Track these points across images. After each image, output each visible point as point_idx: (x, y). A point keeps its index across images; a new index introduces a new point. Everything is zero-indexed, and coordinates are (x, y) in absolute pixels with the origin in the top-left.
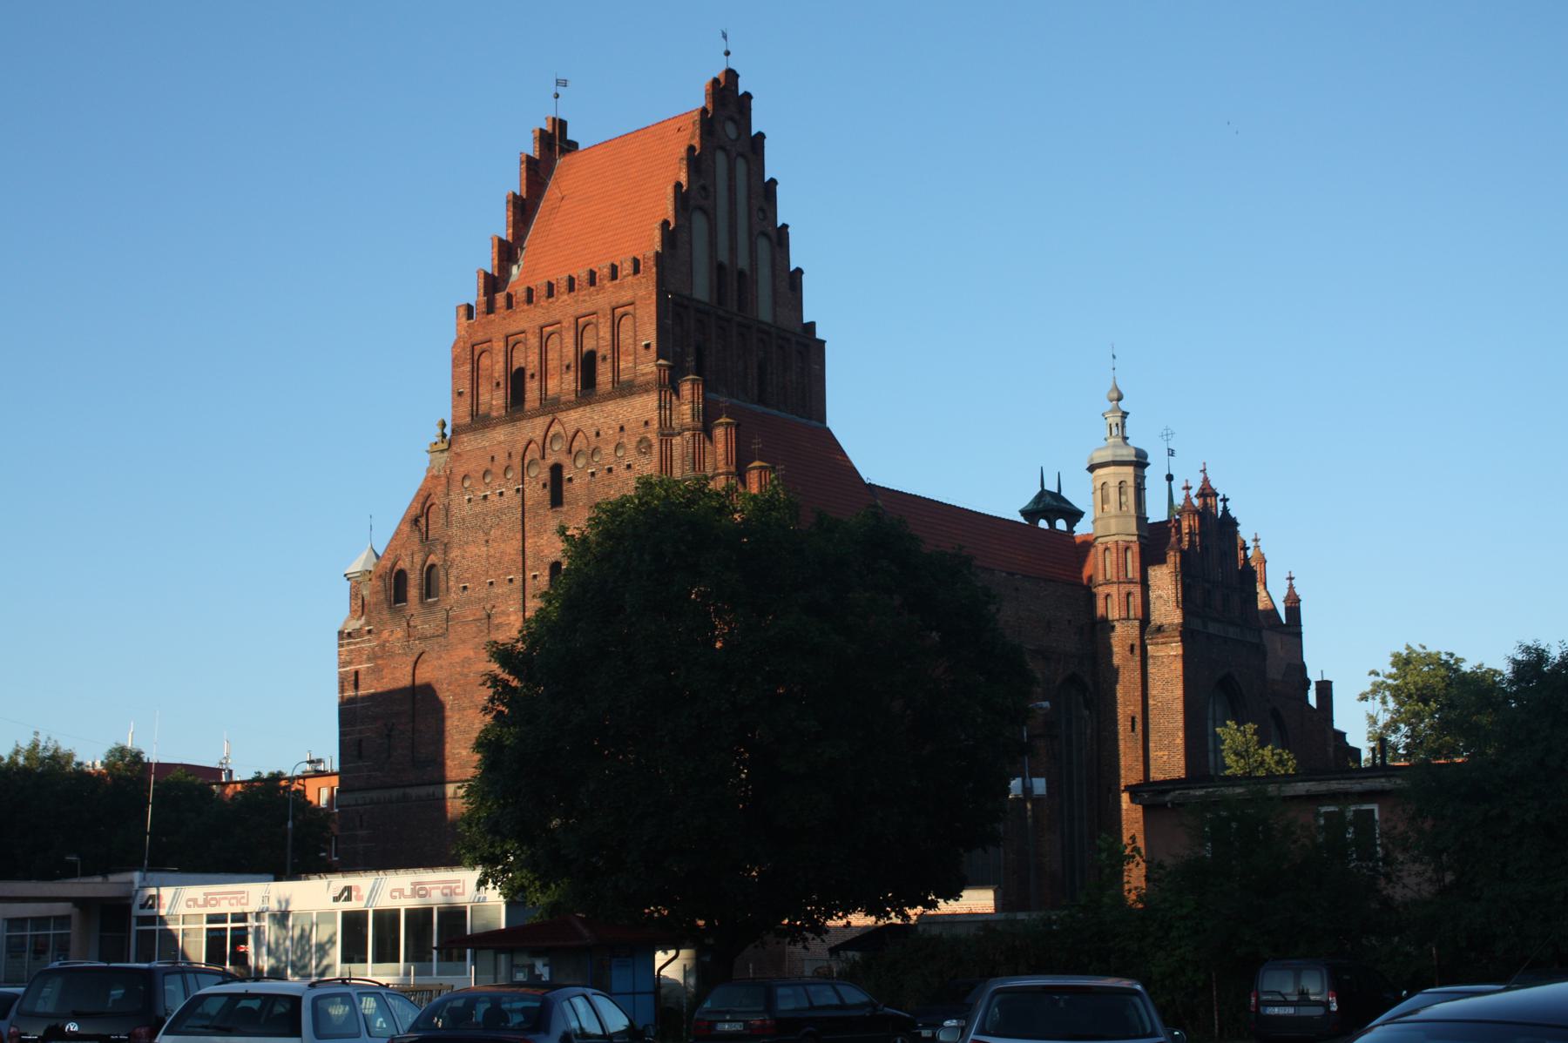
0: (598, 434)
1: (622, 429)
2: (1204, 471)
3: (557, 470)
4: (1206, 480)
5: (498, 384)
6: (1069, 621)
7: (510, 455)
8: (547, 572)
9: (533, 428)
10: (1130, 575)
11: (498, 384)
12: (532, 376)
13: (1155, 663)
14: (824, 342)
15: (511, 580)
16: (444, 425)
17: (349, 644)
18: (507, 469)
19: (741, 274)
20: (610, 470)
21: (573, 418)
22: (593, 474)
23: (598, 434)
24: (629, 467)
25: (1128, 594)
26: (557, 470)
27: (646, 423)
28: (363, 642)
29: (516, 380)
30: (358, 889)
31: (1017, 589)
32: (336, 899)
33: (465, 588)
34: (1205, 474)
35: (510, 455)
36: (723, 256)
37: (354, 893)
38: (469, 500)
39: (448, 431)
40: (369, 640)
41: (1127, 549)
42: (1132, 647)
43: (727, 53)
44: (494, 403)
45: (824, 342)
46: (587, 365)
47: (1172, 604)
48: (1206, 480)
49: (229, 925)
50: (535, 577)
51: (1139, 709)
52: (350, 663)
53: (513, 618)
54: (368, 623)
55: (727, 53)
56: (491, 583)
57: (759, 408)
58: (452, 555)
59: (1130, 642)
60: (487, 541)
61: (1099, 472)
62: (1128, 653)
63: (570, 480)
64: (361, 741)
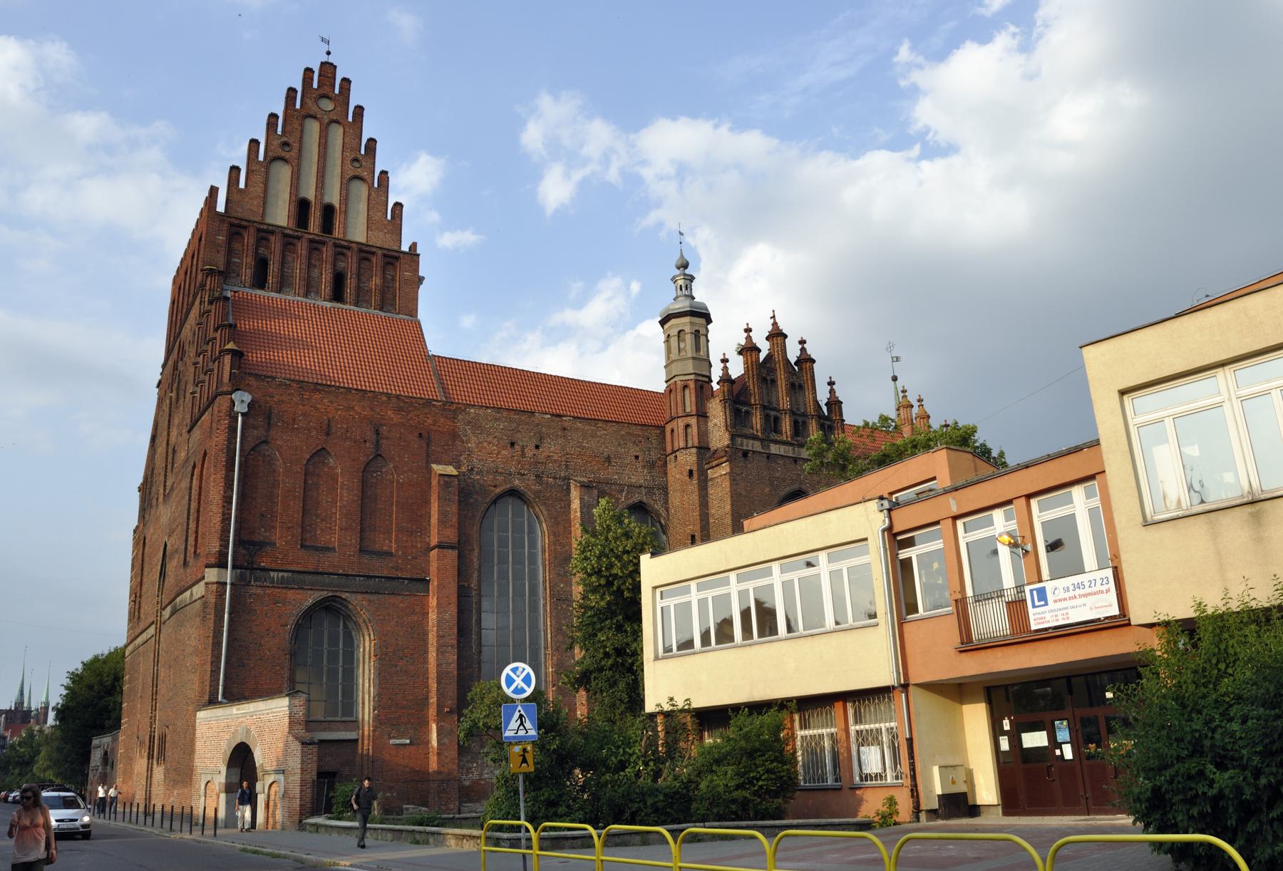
2: (774, 317)
4: (775, 324)
6: (637, 457)
10: (688, 410)
13: (712, 485)
14: (419, 255)
19: (328, 211)
25: (687, 426)
31: (564, 429)
34: (775, 320)
36: (309, 193)
41: (685, 387)
42: (691, 472)
45: (419, 255)
47: (723, 429)
48: (775, 324)
51: (698, 528)
57: (329, 305)
59: (688, 468)
61: (666, 326)
62: (687, 478)
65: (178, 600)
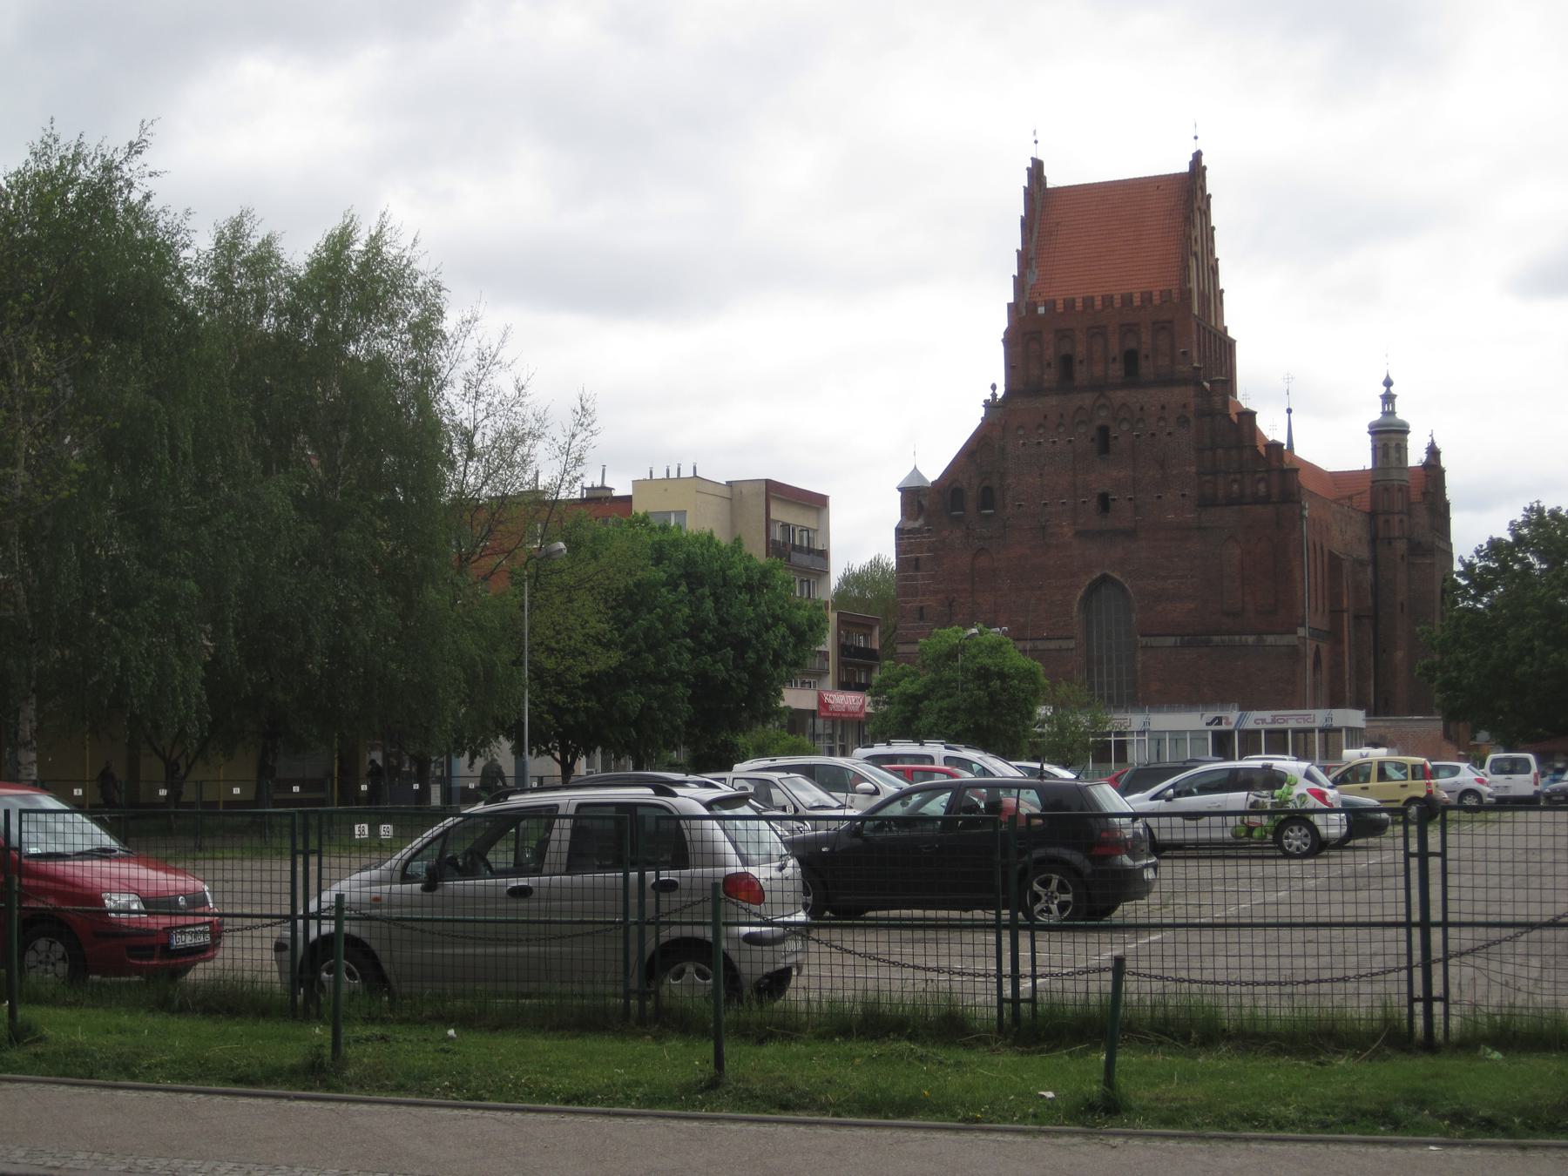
0: (1142, 409)
1: (1163, 407)
3: (1104, 431)
5: (1049, 364)
7: (1062, 416)
8: (1095, 500)
9: (1087, 399)
11: (1049, 364)
12: (1081, 362)
15: (1063, 503)
16: (994, 387)
17: (909, 538)
18: (1059, 425)
20: (1153, 435)
21: (1119, 396)
22: (1138, 436)
23: (1142, 409)
24: (1170, 434)
25: (1401, 521)
26: (1104, 431)
27: (1185, 406)
28: (925, 537)
29: (1067, 362)
30: (1227, 718)
32: (1208, 724)
33: (1020, 505)
35: (1062, 416)
37: (1223, 721)
38: (1024, 444)
39: (1000, 392)
40: (929, 537)
43: (1196, 138)
44: (1046, 377)
46: (1131, 359)
49: (1113, 739)
50: (1084, 502)
52: (911, 552)
53: (1066, 529)
54: (927, 524)
55: (1196, 138)
56: (1046, 504)
58: (1009, 481)
60: (1041, 474)
63: (1116, 438)
64: (922, 608)
65: (1216, 639)
